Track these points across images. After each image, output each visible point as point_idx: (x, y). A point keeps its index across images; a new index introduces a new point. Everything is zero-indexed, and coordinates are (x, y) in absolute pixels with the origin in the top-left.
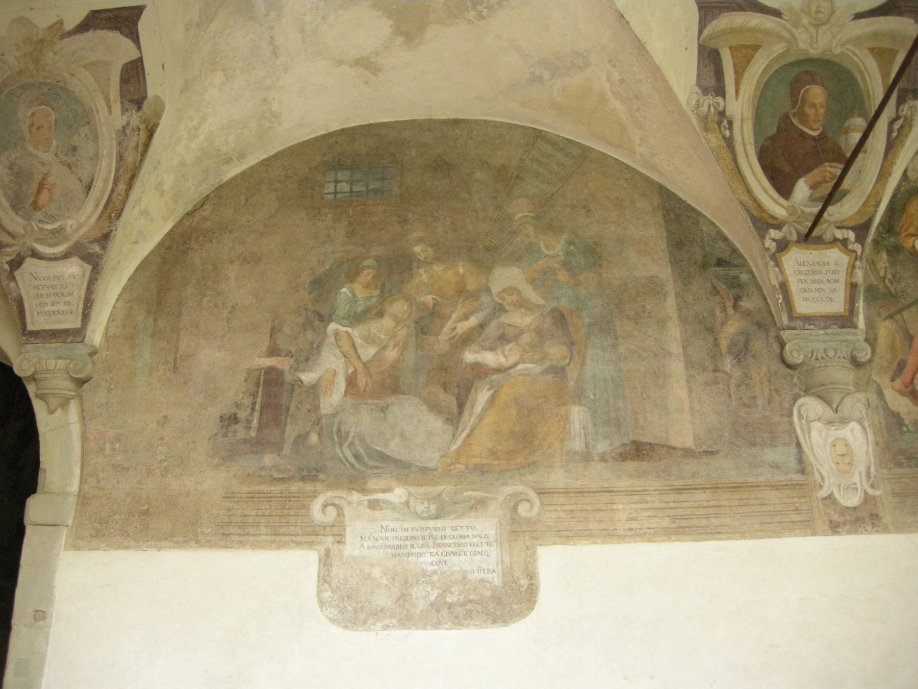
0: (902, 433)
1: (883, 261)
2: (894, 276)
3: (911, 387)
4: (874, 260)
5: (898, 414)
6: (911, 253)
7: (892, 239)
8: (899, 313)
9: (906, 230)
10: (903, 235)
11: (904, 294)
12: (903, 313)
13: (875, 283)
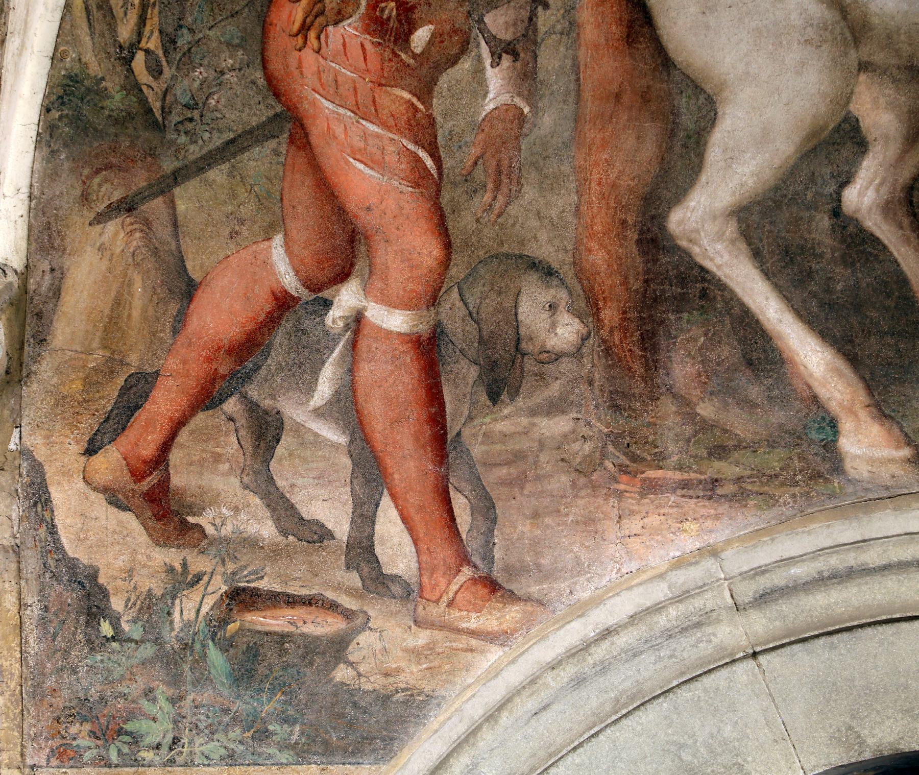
0: (94, 644)
2: (169, 42)
3: (153, 479)
5: (94, 575)
8: (162, 192)
11: (196, 114)
12: (177, 191)
13: (95, 69)
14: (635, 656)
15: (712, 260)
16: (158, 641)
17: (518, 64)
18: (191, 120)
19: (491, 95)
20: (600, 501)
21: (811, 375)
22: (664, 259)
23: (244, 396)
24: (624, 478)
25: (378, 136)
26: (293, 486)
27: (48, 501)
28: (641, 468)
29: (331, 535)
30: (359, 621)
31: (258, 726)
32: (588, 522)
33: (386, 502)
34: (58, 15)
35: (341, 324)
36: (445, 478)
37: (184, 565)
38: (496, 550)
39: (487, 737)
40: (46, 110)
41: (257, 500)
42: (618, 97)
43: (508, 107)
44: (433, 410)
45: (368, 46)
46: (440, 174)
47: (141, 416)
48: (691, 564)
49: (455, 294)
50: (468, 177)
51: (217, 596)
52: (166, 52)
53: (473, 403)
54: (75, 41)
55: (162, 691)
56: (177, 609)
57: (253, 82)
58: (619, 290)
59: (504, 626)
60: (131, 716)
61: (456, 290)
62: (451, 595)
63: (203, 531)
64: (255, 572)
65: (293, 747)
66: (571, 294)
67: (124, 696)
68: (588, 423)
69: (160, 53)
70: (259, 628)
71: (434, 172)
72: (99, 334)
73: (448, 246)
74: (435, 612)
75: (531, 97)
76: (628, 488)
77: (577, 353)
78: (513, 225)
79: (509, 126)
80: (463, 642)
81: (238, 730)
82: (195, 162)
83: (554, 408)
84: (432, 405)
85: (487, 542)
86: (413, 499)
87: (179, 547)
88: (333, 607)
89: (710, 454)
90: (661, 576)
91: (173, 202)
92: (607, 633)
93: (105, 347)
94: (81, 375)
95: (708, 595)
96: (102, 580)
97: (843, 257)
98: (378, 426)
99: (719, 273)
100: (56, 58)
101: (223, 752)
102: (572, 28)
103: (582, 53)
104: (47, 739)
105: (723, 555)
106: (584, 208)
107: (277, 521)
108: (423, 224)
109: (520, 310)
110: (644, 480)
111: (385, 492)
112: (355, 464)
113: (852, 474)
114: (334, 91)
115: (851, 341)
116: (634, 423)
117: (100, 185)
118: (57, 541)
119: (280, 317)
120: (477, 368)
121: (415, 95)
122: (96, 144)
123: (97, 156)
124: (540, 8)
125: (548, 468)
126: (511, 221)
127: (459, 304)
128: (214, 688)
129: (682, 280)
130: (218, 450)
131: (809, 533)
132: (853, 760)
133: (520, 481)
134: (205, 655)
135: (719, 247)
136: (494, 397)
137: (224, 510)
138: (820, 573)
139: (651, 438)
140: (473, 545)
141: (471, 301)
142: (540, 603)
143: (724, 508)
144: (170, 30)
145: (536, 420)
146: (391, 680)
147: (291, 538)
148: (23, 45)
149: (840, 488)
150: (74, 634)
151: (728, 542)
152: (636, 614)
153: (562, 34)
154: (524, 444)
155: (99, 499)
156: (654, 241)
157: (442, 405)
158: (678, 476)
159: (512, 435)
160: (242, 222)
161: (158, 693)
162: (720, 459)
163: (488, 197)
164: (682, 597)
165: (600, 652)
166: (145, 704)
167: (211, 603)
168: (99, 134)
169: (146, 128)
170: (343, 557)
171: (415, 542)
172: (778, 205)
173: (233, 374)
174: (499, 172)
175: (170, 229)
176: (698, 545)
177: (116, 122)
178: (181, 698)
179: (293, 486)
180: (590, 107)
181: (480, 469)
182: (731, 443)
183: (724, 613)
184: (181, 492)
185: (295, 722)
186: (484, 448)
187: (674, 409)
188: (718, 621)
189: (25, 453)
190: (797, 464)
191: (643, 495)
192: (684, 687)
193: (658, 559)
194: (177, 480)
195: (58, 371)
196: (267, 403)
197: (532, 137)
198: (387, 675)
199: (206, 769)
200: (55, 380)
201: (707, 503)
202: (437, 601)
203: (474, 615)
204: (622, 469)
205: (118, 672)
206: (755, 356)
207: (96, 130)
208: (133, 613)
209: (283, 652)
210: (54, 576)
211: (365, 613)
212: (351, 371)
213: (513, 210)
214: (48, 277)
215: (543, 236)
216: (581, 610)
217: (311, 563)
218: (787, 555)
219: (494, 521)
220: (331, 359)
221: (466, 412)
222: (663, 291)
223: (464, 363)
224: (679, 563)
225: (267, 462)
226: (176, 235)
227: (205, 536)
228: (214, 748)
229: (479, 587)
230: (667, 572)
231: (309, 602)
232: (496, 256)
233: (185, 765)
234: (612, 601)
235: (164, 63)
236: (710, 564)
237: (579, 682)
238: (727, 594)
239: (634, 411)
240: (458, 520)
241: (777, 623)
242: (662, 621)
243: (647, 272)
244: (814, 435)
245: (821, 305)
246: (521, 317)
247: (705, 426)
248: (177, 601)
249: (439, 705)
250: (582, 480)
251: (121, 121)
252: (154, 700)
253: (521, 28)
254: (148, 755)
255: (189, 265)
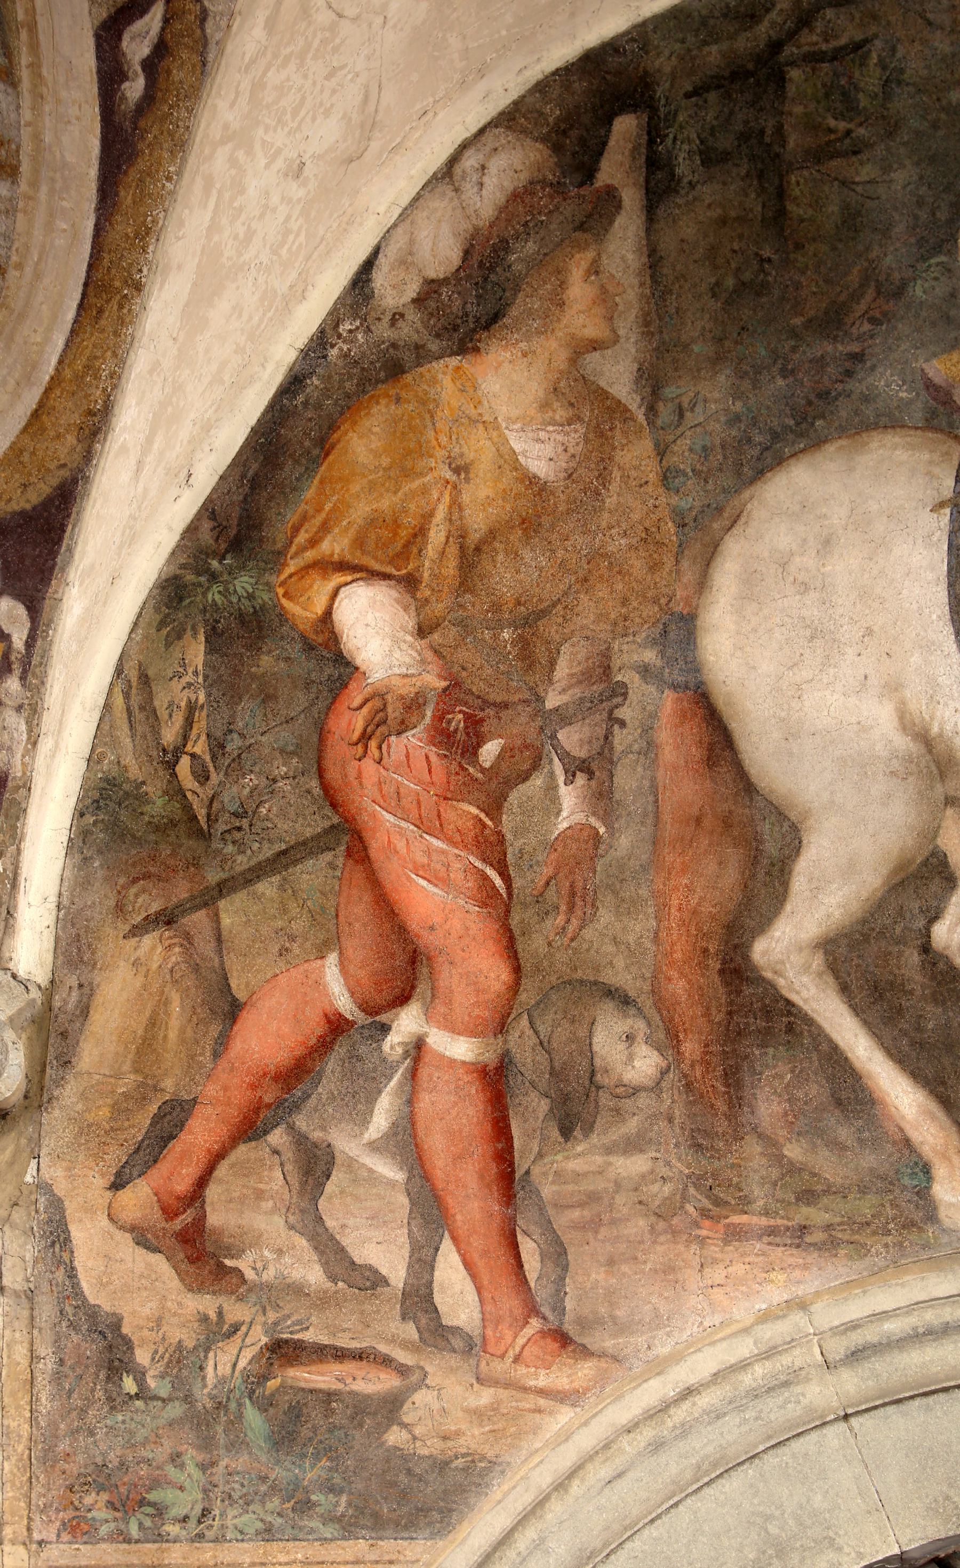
0: (115, 1402)
1: (189, 678)
2: (218, 747)
3: (187, 1217)
4: (151, 673)
5: (116, 1324)
6: (309, 647)
7: (243, 583)
8: (206, 904)
9: (313, 542)
10: (292, 566)
11: (245, 823)
12: (222, 904)
13: (135, 772)
14: (718, 1417)
15: (798, 993)
16: (188, 1399)
17: (593, 783)
18: (239, 829)
19: (564, 814)
20: (681, 1247)
21: (903, 1117)
22: (748, 990)
23: (291, 1127)
24: (707, 1223)
25: (443, 852)
26: (343, 1226)
27: (68, 1240)
28: (724, 1212)
29: (385, 1282)
30: (414, 1378)
31: (299, 1495)
32: (669, 1270)
33: (447, 1245)
34: (96, 716)
35: (400, 1050)
36: (512, 1221)
37: (220, 1314)
38: (567, 1299)
39: (556, 1509)
40: (80, 813)
41: (304, 1242)
42: (698, 821)
43: (583, 827)
44: (500, 1146)
45: (434, 759)
46: (510, 895)
47: (176, 1147)
48: (778, 1318)
49: (524, 1022)
50: (539, 898)
51: (256, 1349)
52: (214, 758)
53: (543, 1139)
54: (115, 743)
55: (191, 1455)
56: (211, 1363)
57: (308, 792)
58: (701, 1021)
59: (576, 1385)
60: (156, 1483)
61: (526, 1017)
62: (518, 1349)
63: (242, 1275)
64: (299, 1322)
65: (339, 1520)
66: (649, 1024)
67: (148, 1462)
68: (668, 1164)
69: (207, 758)
70: (303, 1385)
71: (503, 891)
72: (130, 1056)
73: (517, 970)
74: (499, 1368)
75: (607, 817)
76: (711, 1234)
77: (656, 1088)
78: (588, 950)
79: (583, 846)
80: (531, 1401)
81: (276, 1501)
82: (243, 873)
83: (632, 1146)
84: (499, 1141)
85: (558, 1291)
86: (477, 1243)
87: (214, 1293)
88: (386, 1361)
89: (798, 1199)
90: (746, 1330)
91: (217, 915)
92: (688, 1392)
93: (137, 1071)
94: (109, 1101)
95: (797, 1352)
96: (125, 1330)
97: (934, 994)
98: (440, 1163)
99: (806, 1007)
100: (93, 760)
101: (259, 1525)
102: (650, 748)
103: (660, 774)
104: (58, 1510)
105: (813, 1308)
106: (663, 934)
107: (325, 1265)
108: (491, 947)
109: (595, 1040)
110: (728, 1226)
111: (446, 1234)
112: (413, 1203)
113: (947, 1223)
114: (396, 802)
115: (943, 1083)
116: (717, 1164)
117: (137, 896)
118: (76, 1286)
119: (333, 1042)
120: (548, 1101)
121: (482, 810)
122: (134, 852)
123: (134, 865)
124: (616, 727)
125: (625, 1210)
126: (585, 946)
127: (529, 1032)
128: (250, 1453)
129: (767, 1013)
130: (261, 1186)
131: (903, 1285)
132: (951, 1533)
133: (595, 1224)
134: (240, 1416)
135: (805, 979)
136: (566, 1132)
137: (266, 1253)
138: (915, 1329)
139: (735, 1180)
140: (542, 1293)
141: (541, 1029)
142: (615, 1359)
143: (812, 1257)
144: (219, 734)
145: (612, 1159)
146: (450, 1444)
147: (340, 1284)
148: (57, 746)
149: (935, 1238)
150: (93, 1391)
151: (818, 1294)
152: (719, 1371)
153: (639, 753)
154: (600, 1185)
155: (126, 1239)
156: (737, 971)
157: (510, 1139)
158: (764, 1221)
159: (585, 1174)
160: (292, 938)
161: (187, 1459)
162: (808, 1204)
163: (560, 920)
164: (770, 1353)
165: (680, 1414)
166: (171, 1470)
167: (249, 1356)
168: (138, 841)
169: (189, 836)
170: (398, 1306)
171: (479, 1290)
172: (866, 938)
173: (280, 1103)
174: (573, 894)
175: (213, 944)
176: (786, 1297)
177: (157, 829)
178: (213, 1464)
179: (343, 1226)
180: (670, 830)
181: (551, 1211)
182: (819, 1188)
183: (813, 1372)
184: (218, 1232)
185: (341, 1491)
186: (555, 1188)
187: (759, 1149)
188: (807, 1380)
189: (43, 1187)
190: (890, 1212)
191: (726, 1242)
192: (771, 1452)
193: (743, 1312)
194: (214, 1219)
195: (83, 1096)
196: (316, 1135)
197: (607, 859)
198: (445, 1438)
199: (240, 1545)
200: (79, 1107)
201: (794, 1251)
202: (502, 1356)
203: (542, 1372)
204: (704, 1213)
205: (142, 1433)
206: (844, 1095)
207: (134, 837)
208: (160, 1367)
209: (329, 1412)
210: (71, 1325)
211: (422, 1368)
212: (410, 1102)
213: (587, 933)
214: (75, 994)
215: (620, 963)
216: (659, 1367)
217: (362, 1313)
218: (879, 1309)
219: (565, 1268)
220: (388, 1089)
221: (536, 1149)
222: (747, 1024)
223: (534, 1095)
224: (765, 1317)
225: (315, 1200)
226: (220, 952)
227: (244, 1281)
228: (249, 1521)
229: (549, 1340)
230: (752, 1325)
231: (360, 1356)
232: (570, 982)
233: (216, 1540)
234: (694, 1357)
235: (212, 769)
236: (798, 1318)
237: (657, 1446)
238: (817, 1351)
239: (718, 1151)
240: (526, 1267)
241: (870, 1383)
242: (747, 1380)
243: (731, 1003)
244: (906, 1181)
245: (913, 1044)
246: (596, 1048)
247: (793, 1169)
248: (211, 1355)
249: (503, 1472)
250: (661, 1225)
251: (162, 828)
252: (182, 1466)
253: (596, 746)
254: (173, 1529)
255: (233, 983)
